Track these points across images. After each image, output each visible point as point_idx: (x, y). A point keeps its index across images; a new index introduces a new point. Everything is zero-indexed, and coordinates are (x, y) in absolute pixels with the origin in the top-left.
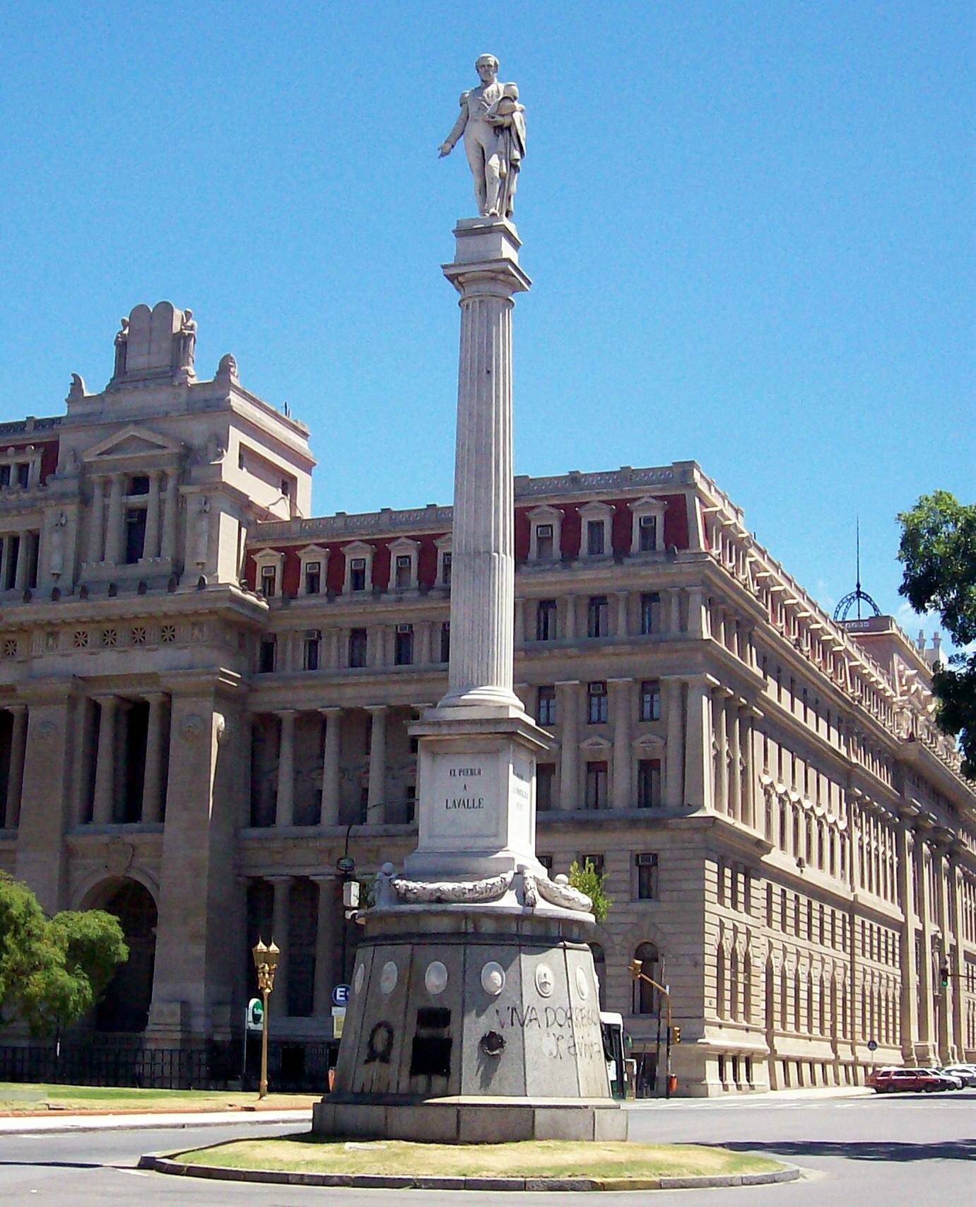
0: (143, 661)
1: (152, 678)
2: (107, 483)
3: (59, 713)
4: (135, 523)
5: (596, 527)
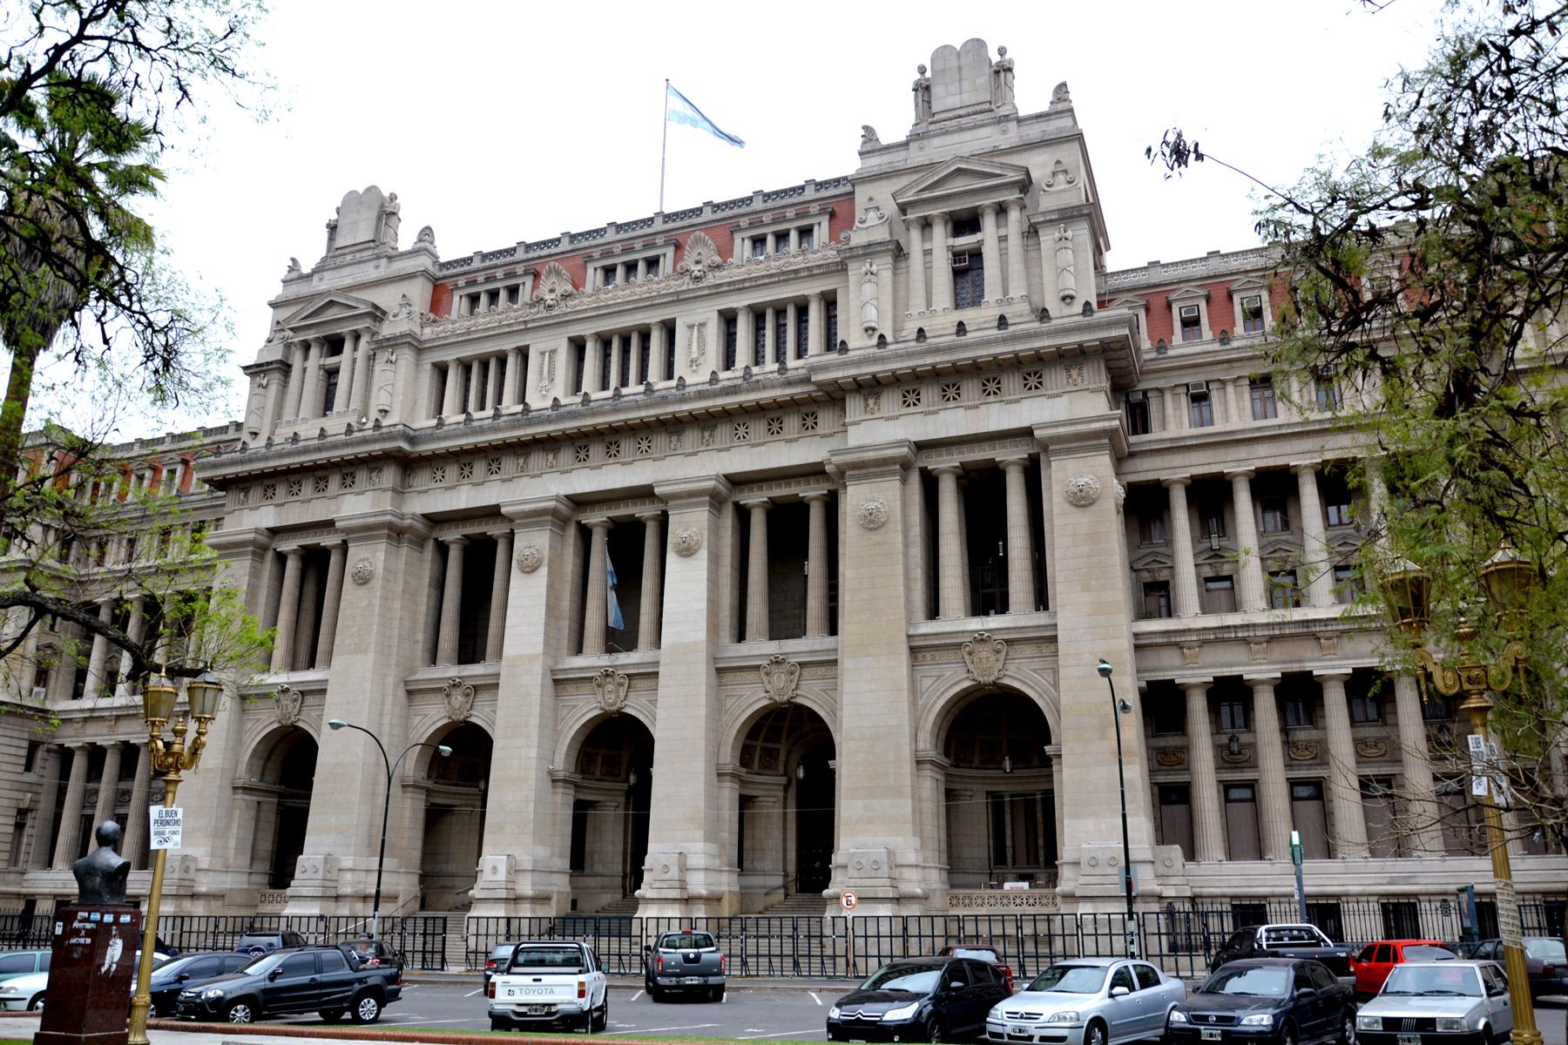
4: (967, 268)
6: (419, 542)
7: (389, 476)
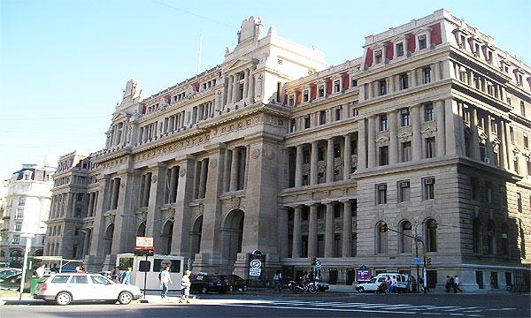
3: (217, 156)
5: (400, 46)
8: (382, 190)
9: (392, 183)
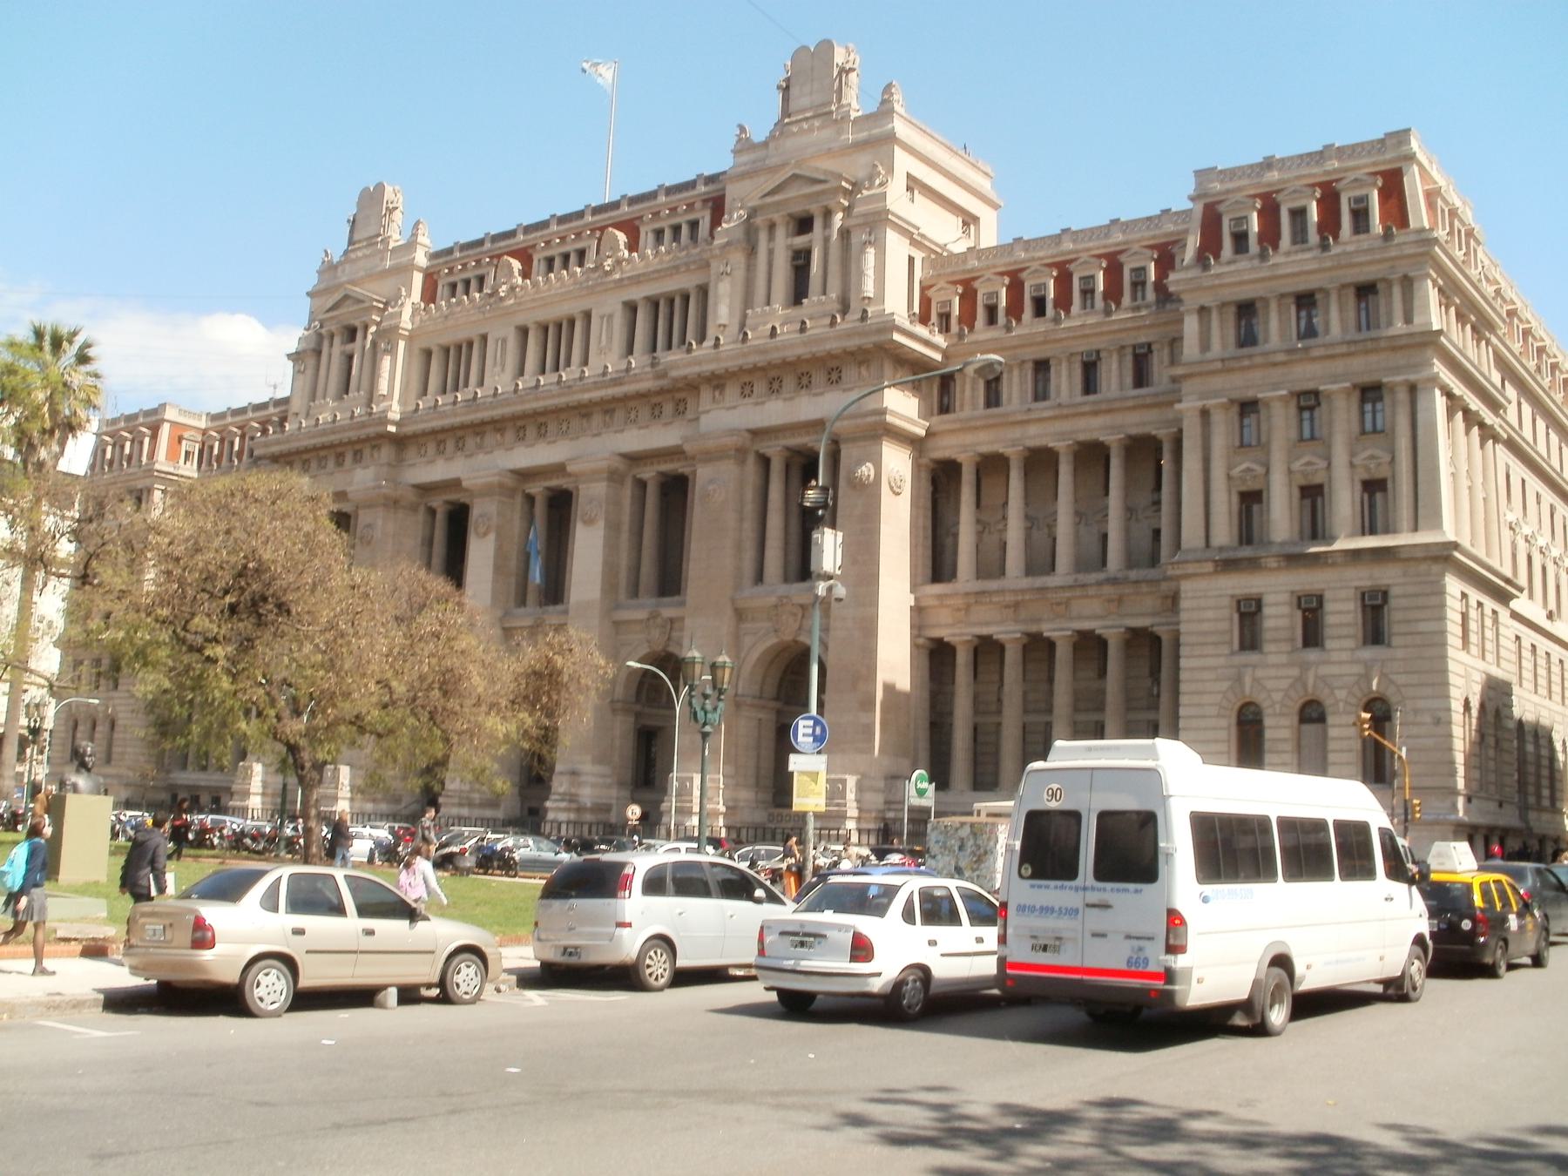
0: (806, 407)
1: (818, 425)
2: (772, 227)
6: (414, 508)
7: (386, 453)
8: (1249, 613)
9: (1276, 590)
